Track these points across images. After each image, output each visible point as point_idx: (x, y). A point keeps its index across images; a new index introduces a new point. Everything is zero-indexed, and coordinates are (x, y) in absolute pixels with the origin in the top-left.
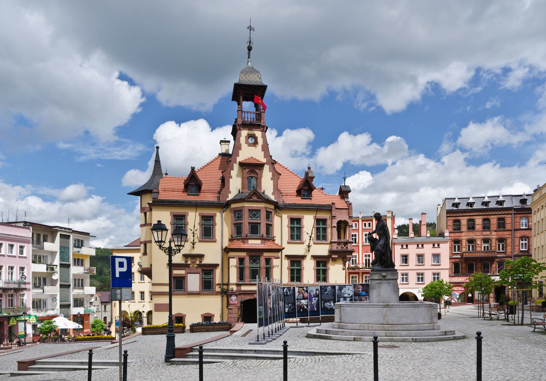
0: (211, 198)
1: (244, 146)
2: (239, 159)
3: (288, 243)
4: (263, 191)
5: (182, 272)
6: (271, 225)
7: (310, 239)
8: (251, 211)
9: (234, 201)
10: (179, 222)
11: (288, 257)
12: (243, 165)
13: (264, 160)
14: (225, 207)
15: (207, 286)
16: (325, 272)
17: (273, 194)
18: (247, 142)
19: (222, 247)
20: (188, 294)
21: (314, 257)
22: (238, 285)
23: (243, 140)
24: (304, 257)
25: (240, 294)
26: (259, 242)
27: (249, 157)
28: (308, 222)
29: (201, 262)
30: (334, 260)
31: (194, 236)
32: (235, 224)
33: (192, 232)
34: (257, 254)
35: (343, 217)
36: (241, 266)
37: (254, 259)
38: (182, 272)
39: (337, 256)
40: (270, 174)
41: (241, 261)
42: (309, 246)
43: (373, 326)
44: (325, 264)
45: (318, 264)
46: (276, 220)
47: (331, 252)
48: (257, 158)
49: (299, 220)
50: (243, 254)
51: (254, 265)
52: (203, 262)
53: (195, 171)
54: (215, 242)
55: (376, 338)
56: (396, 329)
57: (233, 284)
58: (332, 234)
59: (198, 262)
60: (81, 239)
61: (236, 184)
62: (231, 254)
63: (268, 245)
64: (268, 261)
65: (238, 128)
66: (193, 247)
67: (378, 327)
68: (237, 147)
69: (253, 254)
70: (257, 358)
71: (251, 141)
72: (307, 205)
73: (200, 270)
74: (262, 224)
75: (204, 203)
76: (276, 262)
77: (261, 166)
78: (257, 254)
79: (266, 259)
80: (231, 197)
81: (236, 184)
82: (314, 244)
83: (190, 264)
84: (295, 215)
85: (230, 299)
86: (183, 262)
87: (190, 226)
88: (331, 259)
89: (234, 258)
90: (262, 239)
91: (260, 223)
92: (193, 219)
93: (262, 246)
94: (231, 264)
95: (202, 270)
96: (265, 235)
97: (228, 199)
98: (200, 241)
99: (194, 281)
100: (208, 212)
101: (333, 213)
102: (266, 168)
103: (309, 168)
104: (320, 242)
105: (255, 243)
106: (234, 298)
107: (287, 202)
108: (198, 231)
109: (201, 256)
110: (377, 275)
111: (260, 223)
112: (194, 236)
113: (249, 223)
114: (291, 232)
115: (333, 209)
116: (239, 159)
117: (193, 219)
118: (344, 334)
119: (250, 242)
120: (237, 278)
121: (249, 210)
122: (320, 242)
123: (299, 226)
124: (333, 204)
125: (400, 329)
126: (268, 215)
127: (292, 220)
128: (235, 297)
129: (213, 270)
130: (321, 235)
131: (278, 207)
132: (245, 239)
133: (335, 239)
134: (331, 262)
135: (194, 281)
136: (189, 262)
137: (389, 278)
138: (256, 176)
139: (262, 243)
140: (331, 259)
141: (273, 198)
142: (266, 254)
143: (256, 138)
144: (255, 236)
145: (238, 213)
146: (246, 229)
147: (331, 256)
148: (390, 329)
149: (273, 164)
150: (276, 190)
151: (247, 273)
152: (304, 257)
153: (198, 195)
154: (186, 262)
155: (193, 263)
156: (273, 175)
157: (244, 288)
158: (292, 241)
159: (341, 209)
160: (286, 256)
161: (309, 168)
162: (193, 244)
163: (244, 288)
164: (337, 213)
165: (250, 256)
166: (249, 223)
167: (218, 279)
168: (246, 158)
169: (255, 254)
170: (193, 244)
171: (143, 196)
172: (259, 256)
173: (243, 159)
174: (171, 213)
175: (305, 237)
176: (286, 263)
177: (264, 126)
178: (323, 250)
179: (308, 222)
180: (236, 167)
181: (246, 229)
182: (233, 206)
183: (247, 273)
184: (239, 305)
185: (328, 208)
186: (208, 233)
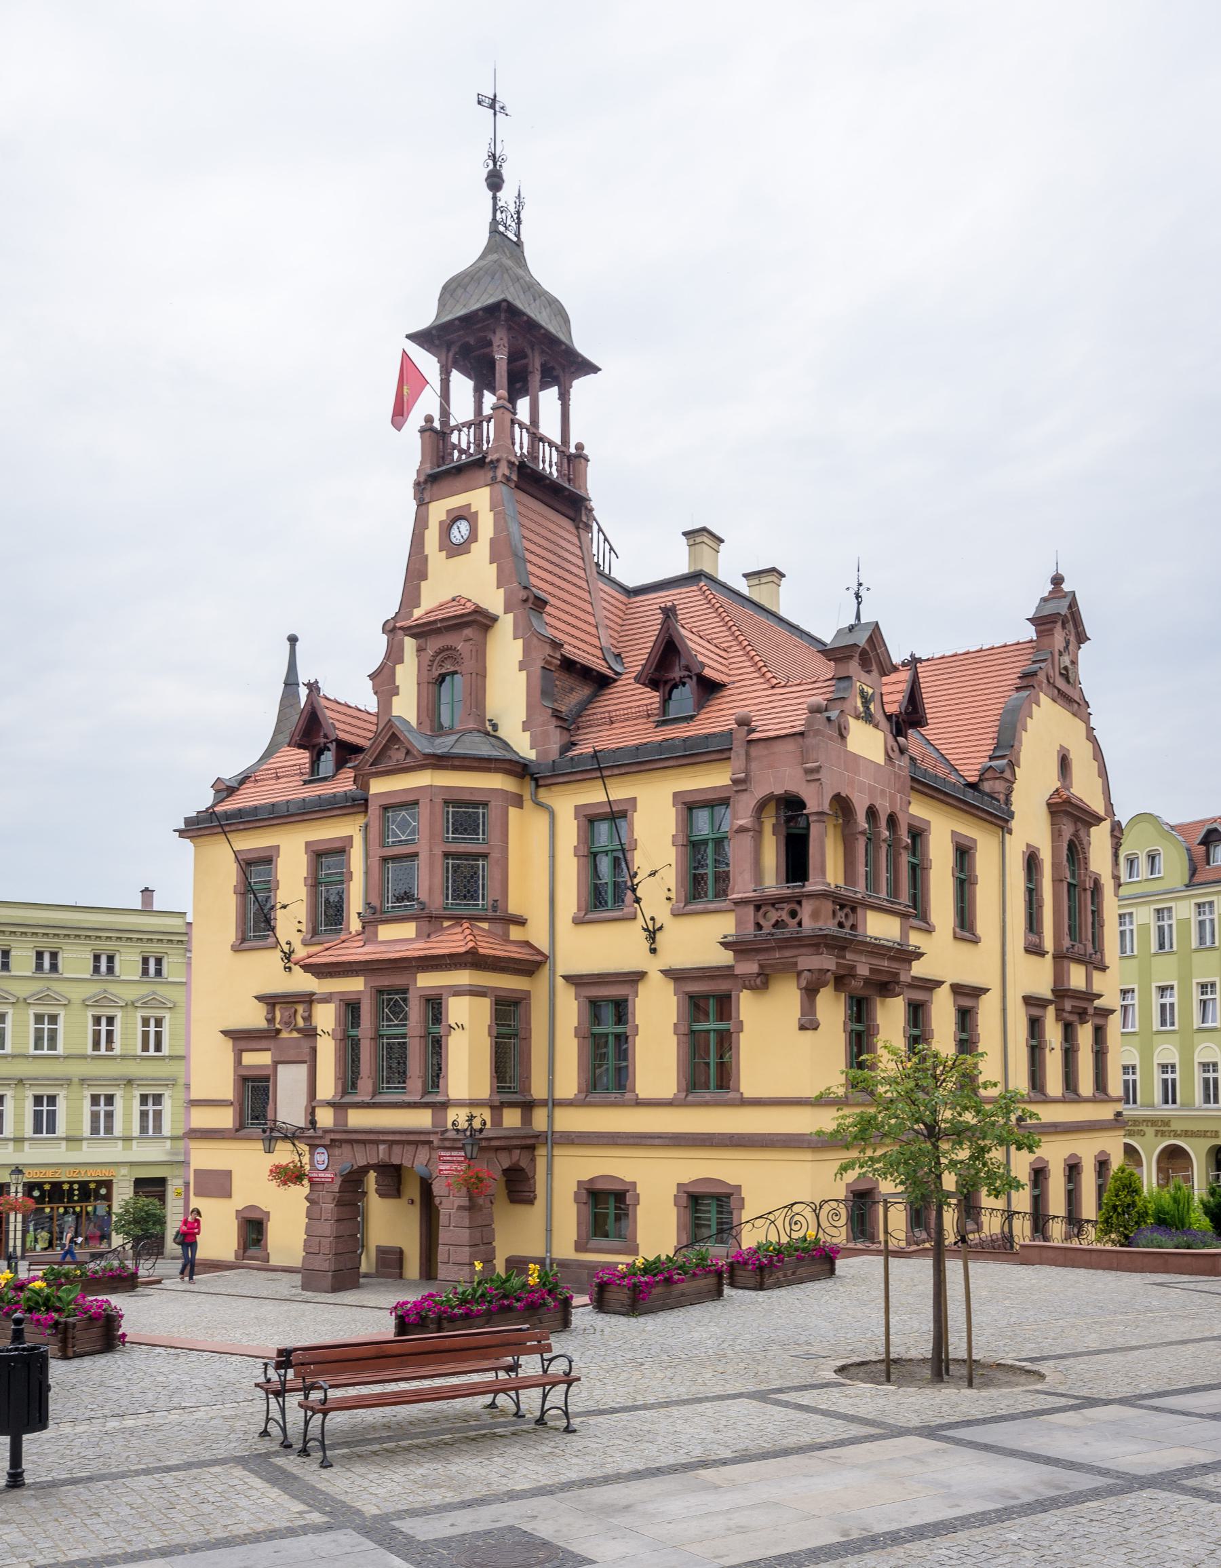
3: (578, 922)
11: (574, 980)
13: (494, 601)
16: (726, 1041)
17: (526, 726)
22: (339, 1107)
24: (636, 978)
26: (407, 930)
30: (762, 982)
35: (782, 776)
40: (515, 649)
44: (724, 1005)
50: (355, 985)
58: (759, 864)
69: (385, 981)
71: (461, 531)
74: (421, 856)
76: (458, 1010)
77: (481, 621)
84: (593, 795)
86: (261, 1023)
93: (421, 948)
105: (399, 936)
121: (385, 808)
126: (466, 815)
133: (772, 880)
152: (636, 978)
154: (271, 1020)
156: (527, 650)
160: (566, 978)
163: (358, 1119)
176: (569, 1009)
178: (702, 940)
184: (336, 1188)
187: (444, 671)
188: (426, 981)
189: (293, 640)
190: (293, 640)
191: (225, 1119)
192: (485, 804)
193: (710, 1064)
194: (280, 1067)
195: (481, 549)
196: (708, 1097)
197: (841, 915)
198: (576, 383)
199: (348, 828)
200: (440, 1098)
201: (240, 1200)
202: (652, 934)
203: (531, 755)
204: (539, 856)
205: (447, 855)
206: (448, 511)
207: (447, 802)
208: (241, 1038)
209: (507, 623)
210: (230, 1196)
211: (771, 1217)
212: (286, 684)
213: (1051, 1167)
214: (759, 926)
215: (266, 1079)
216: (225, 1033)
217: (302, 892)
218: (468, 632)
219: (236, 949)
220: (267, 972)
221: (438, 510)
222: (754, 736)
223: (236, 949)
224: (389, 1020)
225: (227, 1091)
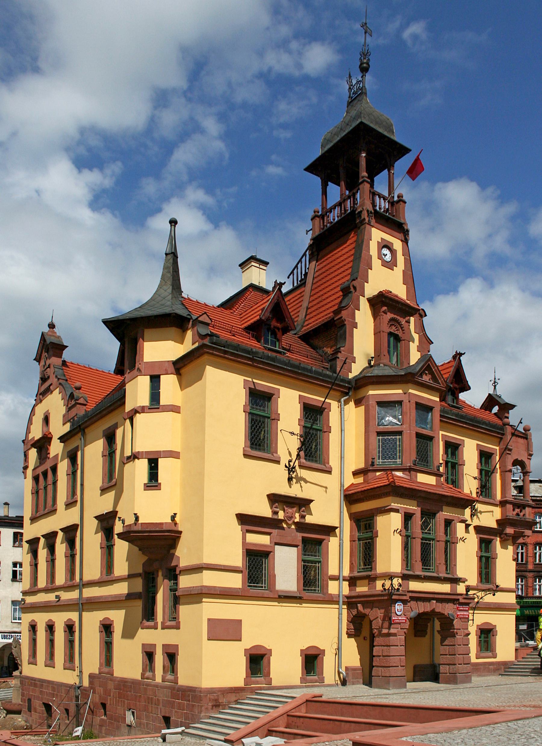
15: (312, 580)
19: (342, 485)
29: (303, 517)
45: (482, 542)
52: (309, 519)
54: (329, 472)
63: (447, 491)
80: (356, 369)
83: (281, 521)
97: (351, 376)
99: (286, 566)
106: (399, 607)
128: (402, 607)
135: (286, 566)
142: (446, 513)
180: (364, 304)
184: (407, 626)
186: (313, 448)
191: (235, 581)
194: (277, 547)
197: (517, 510)
201: (249, 640)
213: (56, 625)
220: (270, 478)
225: (237, 559)
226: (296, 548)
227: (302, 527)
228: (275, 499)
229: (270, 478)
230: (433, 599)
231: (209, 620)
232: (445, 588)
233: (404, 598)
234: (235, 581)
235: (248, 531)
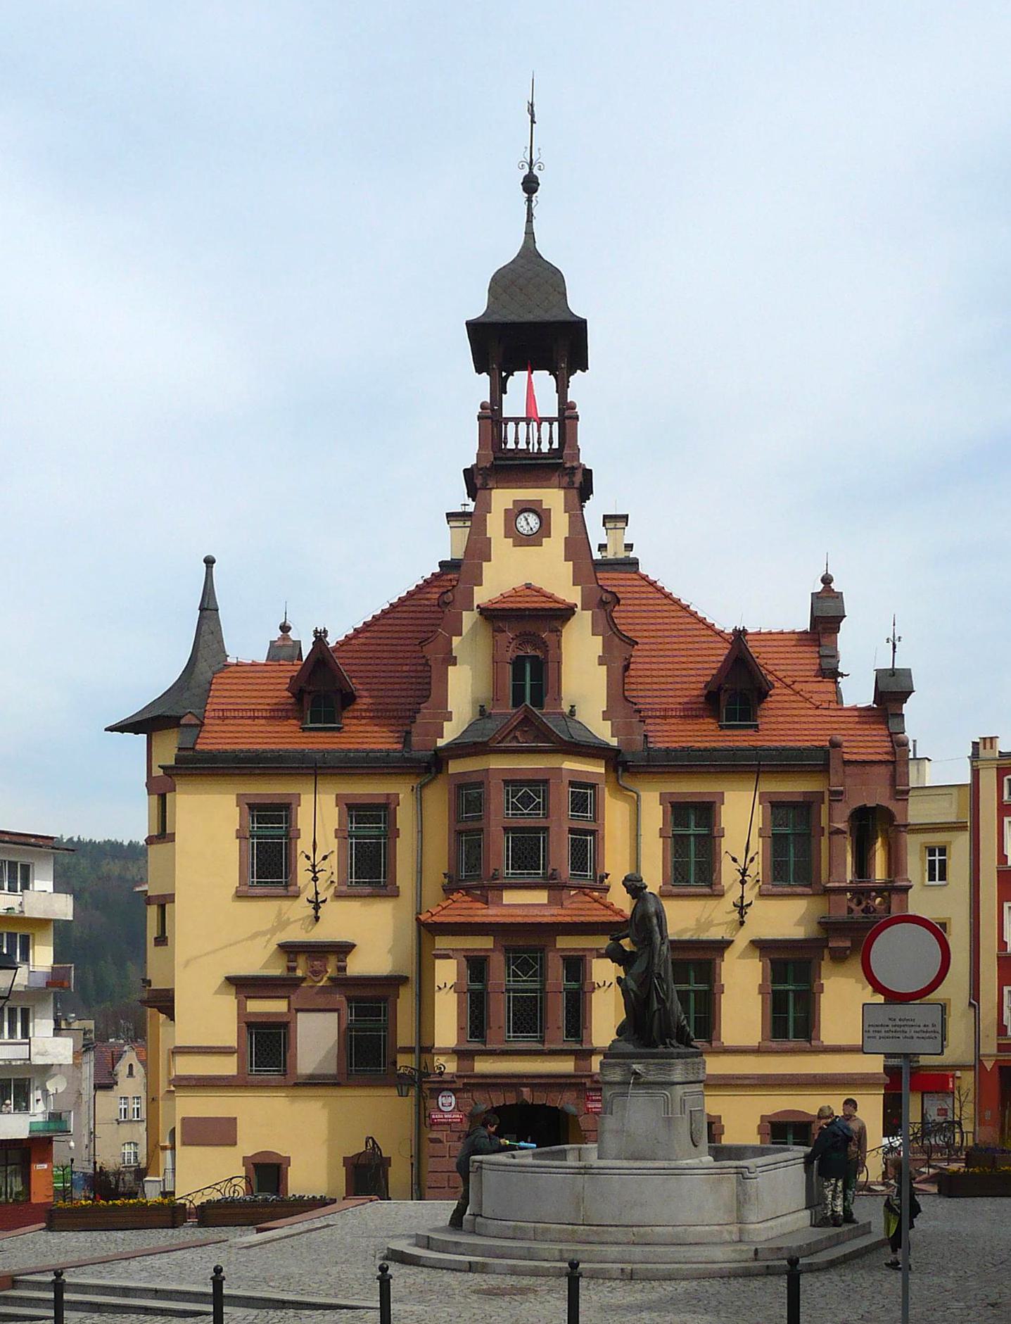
0: (379, 740)
1: (500, 544)
2: (483, 595)
4: (566, 709)
5: (278, 1006)
6: (593, 833)
7: (743, 882)
8: (513, 783)
9: (460, 749)
10: (273, 829)
12: (491, 615)
13: (571, 594)
14: (428, 770)
18: (511, 530)
20: (296, 1085)
21: (762, 947)
23: (495, 525)
24: (722, 946)
25: (468, 1088)
26: (541, 897)
27: (518, 583)
28: (741, 816)
29: (344, 969)
30: (839, 957)
31: (315, 879)
32: (460, 833)
33: (308, 864)
34: (534, 942)
35: (876, 794)
36: (477, 986)
37: (525, 961)
38: (278, 1006)
39: (848, 944)
41: (476, 966)
42: (742, 908)
43: (548, 1230)
46: (614, 813)
47: (828, 927)
48: (548, 589)
49: (706, 811)
50: (484, 943)
51: (527, 984)
53: (325, 644)
55: (574, 1265)
56: (611, 1239)
57: (443, 1052)
59: (331, 970)
60: (21, 860)
61: (464, 688)
62: (443, 943)
64: (576, 967)
65: (479, 482)
66: (317, 918)
67: (560, 1231)
68: (478, 550)
70: (147, 1311)
71: (528, 523)
72: (734, 752)
73: (340, 999)
75: (351, 760)
78: (534, 942)
79: (565, 959)
80: (451, 732)
81: (464, 688)
82: (762, 895)
83: (303, 979)
85: (430, 1103)
87: (303, 845)
88: (826, 952)
89: (448, 957)
90: (553, 885)
91: (546, 829)
92: (319, 818)
94: (439, 981)
95: (349, 1000)
96: (566, 871)
97: (441, 743)
98: (339, 896)
99: (317, 1038)
100: (368, 789)
101: (834, 779)
102: (583, 621)
103: (827, 580)
104: (787, 890)
105: (525, 902)
106: (447, 1102)
107: (659, 743)
108: (334, 860)
109: (344, 949)
110: (618, 1070)
111: (546, 829)
112: (315, 879)
113: (506, 830)
114: (676, 853)
115: (834, 763)
116: (483, 595)
117: (319, 818)
118: (461, 1250)
119: (510, 897)
120: (461, 1029)
121: (507, 783)
122: (787, 890)
123: (703, 831)
124: (835, 745)
125: (621, 1238)
126: (584, 797)
127: (679, 811)
129: (385, 999)
130: (790, 861)
131: (624, 765)
132: (488, 889)
134: (826, 966)
136: (299, 973)
137: (651, 1079)
138: (538, 653)
139: (551, 902)
140: (826, 952)
141: (604, 732)
143: (544, 516)
144: (526, 876)
145: (469, 798)
146: (499, 848)
147: (827, 940)
148: (591, 1239)
149: (602, 604)
150: (622, 699)
151: (499, 1010)
152: (722, 946)
153: (339, 729)
155: (315, 973)
157: (483, 1066)
158: (675, 890)
159: (864, 763)
161: (827, 580)
162: (317, 907)
163: (483, 1066)
164: (848, 781)
165: (507, 950)
166: (506, 830)
167: (405, 1034)
168: (507, 588)
169: (527, 943)
170: (317, 907)
171: (157, 737)
172: (542, 950)
173: (495, 595)
174: (240, 797)
175: (728, 873)
177: (573, 468)
179: (741, 816)
181: (499, 848)
182: (455, 767)
183: (499, 1010)
185: (816, 760)
187: (522, 653)
188: (564, 942)
189: (209, 562)
190: (209, 562)
192: (593, 786)
193: (791, 1016)
194: (299, 1015)
195: (555, 544)
196: (791, 1045)
198: (571, 378)
199: (402, 790)
200: (584, 1047)
202: (742, 908)
203: (614, 742)
204: (633, 835)
205: (571, 831)
206: (514, 501)
207: (572, 784)
208: (243, 986)
209: (583, 621)
210: (235, 1144)
211: (218, 1187)
212: (202, 609)
214: (850, 910)
215: (285, 1025)
216: (231, 981)
217: (329, 844)
218: (556, 624)
219: (240, 896)
221: (502, 498)
222: (847, 757)
223: (240, 896)
224: (516, 975)
226: (336, 1015)
227: (343, 983)
228: (290, 950)
229: (288, 920)
230: (525, 1085)
231: (183, 1119)
232: (566, 1066)
233: (454, 1086)
234: (228, 1067)
235: (248, 997)
